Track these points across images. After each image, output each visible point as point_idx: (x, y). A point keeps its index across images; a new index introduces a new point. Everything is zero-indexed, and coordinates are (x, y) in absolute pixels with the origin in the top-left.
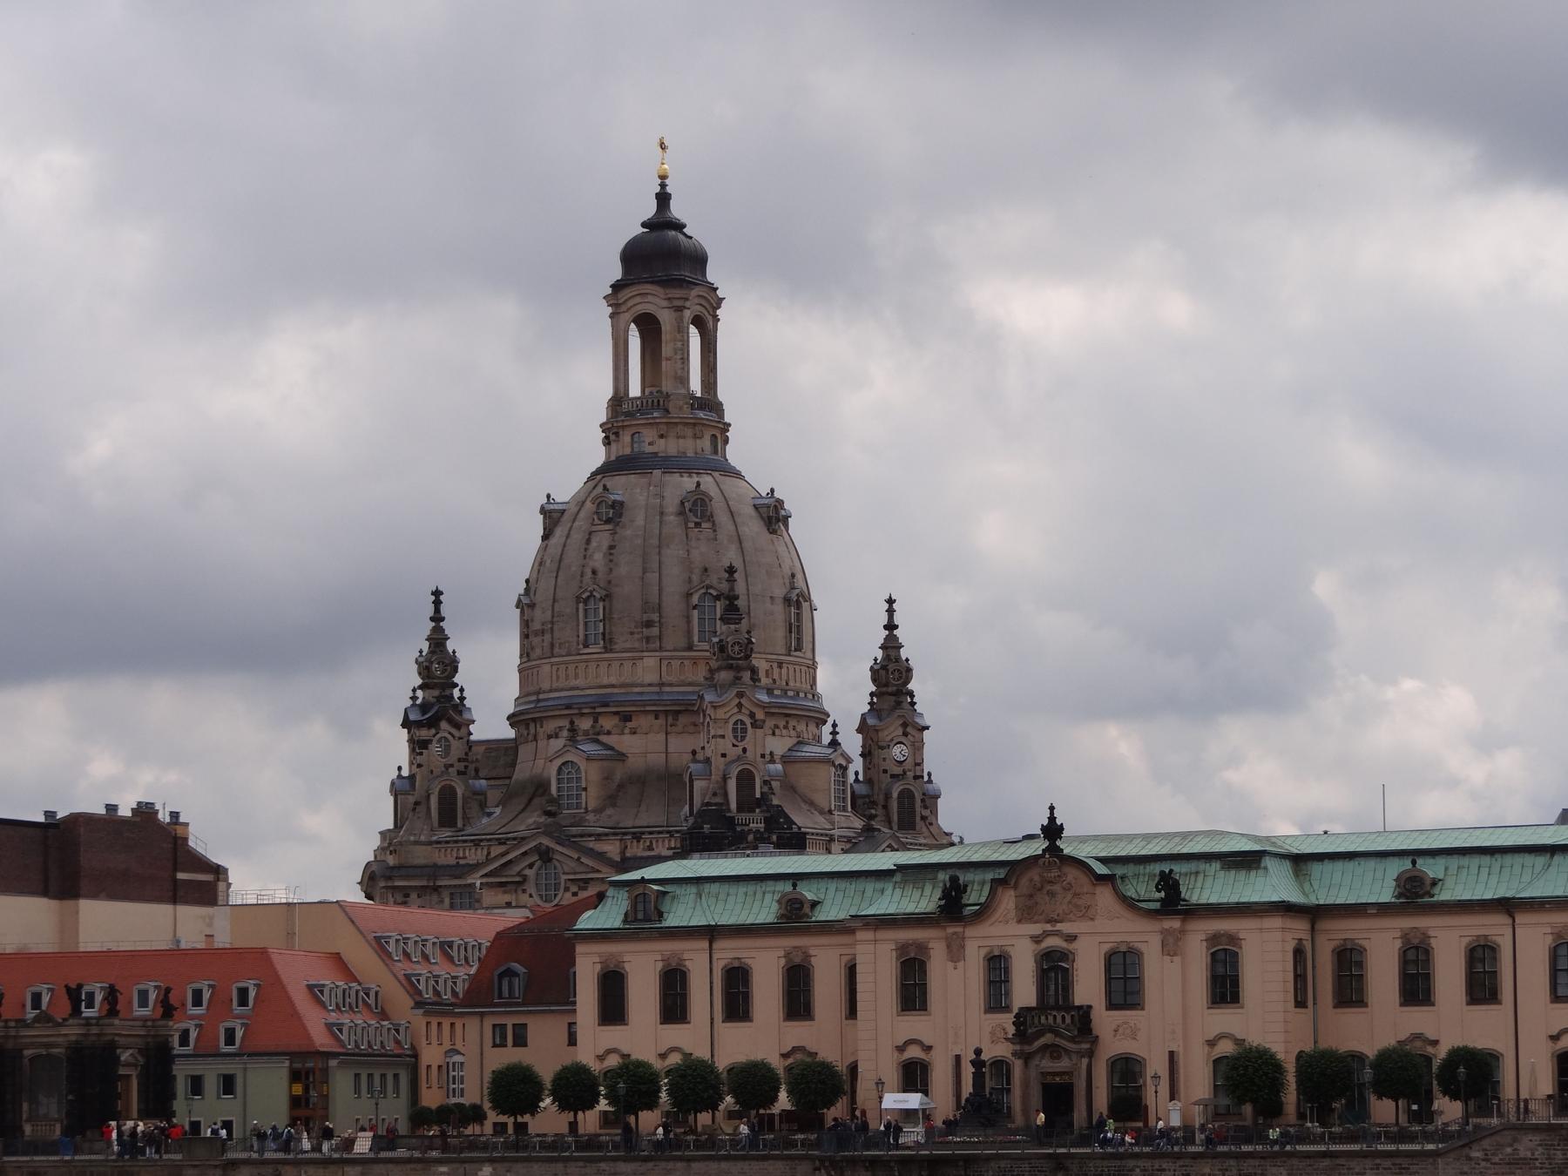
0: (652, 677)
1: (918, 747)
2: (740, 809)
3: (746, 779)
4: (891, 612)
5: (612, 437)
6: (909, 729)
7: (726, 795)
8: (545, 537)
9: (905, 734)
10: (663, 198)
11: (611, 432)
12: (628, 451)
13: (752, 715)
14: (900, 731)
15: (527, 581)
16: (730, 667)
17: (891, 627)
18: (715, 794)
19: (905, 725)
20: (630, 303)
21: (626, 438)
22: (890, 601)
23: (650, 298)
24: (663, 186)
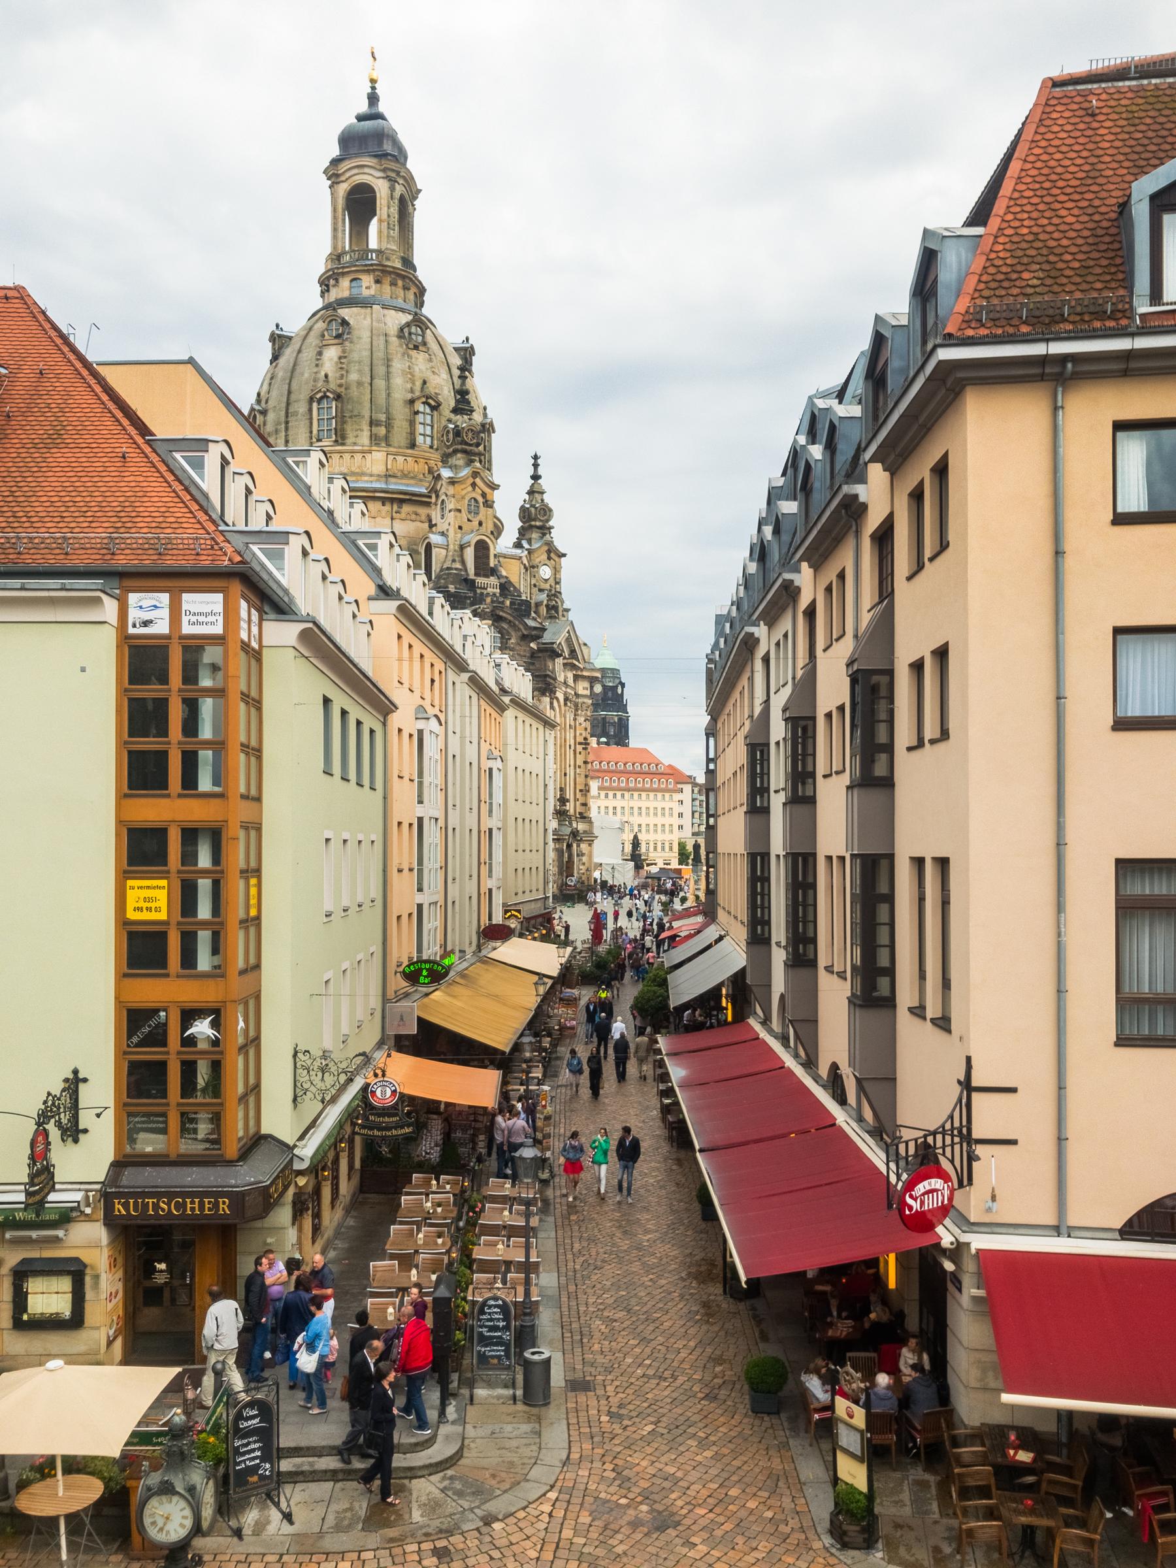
0: (379, 469)
1: (556, 570)
2: (476, 574)
3: (482, 549)
4: (536, 466)
5: (332, 282)
6: (552, 555)
7: (463, 562)
8: (275, 358)
9: (549, 558)
10: (373, 99)
11: (325, 283)
12: (346, 294)
13: (484, 495)
14: (545, 556)
15: (259, 395)
16: (465, 452)
17: (536, 477)
18: (454, 561)
19: (549, 552)
20: (348, 175)
21: (345, 283)
22: (536, 457)
23: (366, 170)
24: (373, 88)
